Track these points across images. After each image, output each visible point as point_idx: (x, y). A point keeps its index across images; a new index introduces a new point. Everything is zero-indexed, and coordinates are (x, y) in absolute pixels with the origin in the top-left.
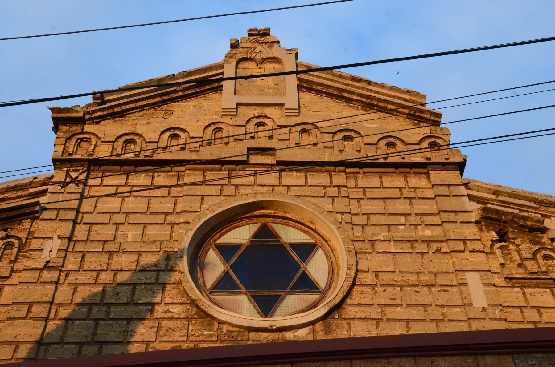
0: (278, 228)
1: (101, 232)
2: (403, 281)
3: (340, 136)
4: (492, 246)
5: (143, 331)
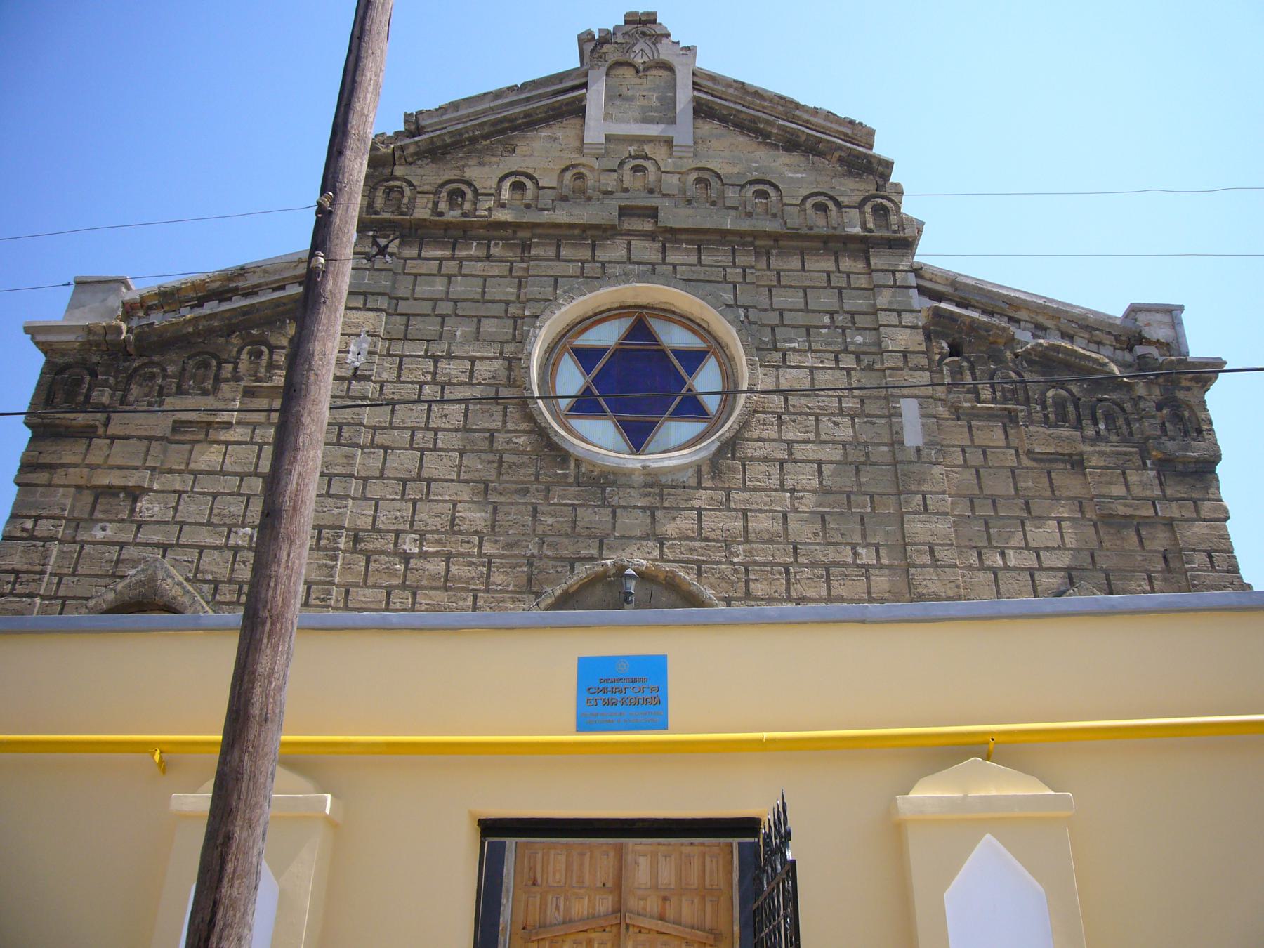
0: (657, 326)
1: (421, 327)
2: (819, 408)
3: (750, 190)
4: (942, 359)
5: (480, 466)
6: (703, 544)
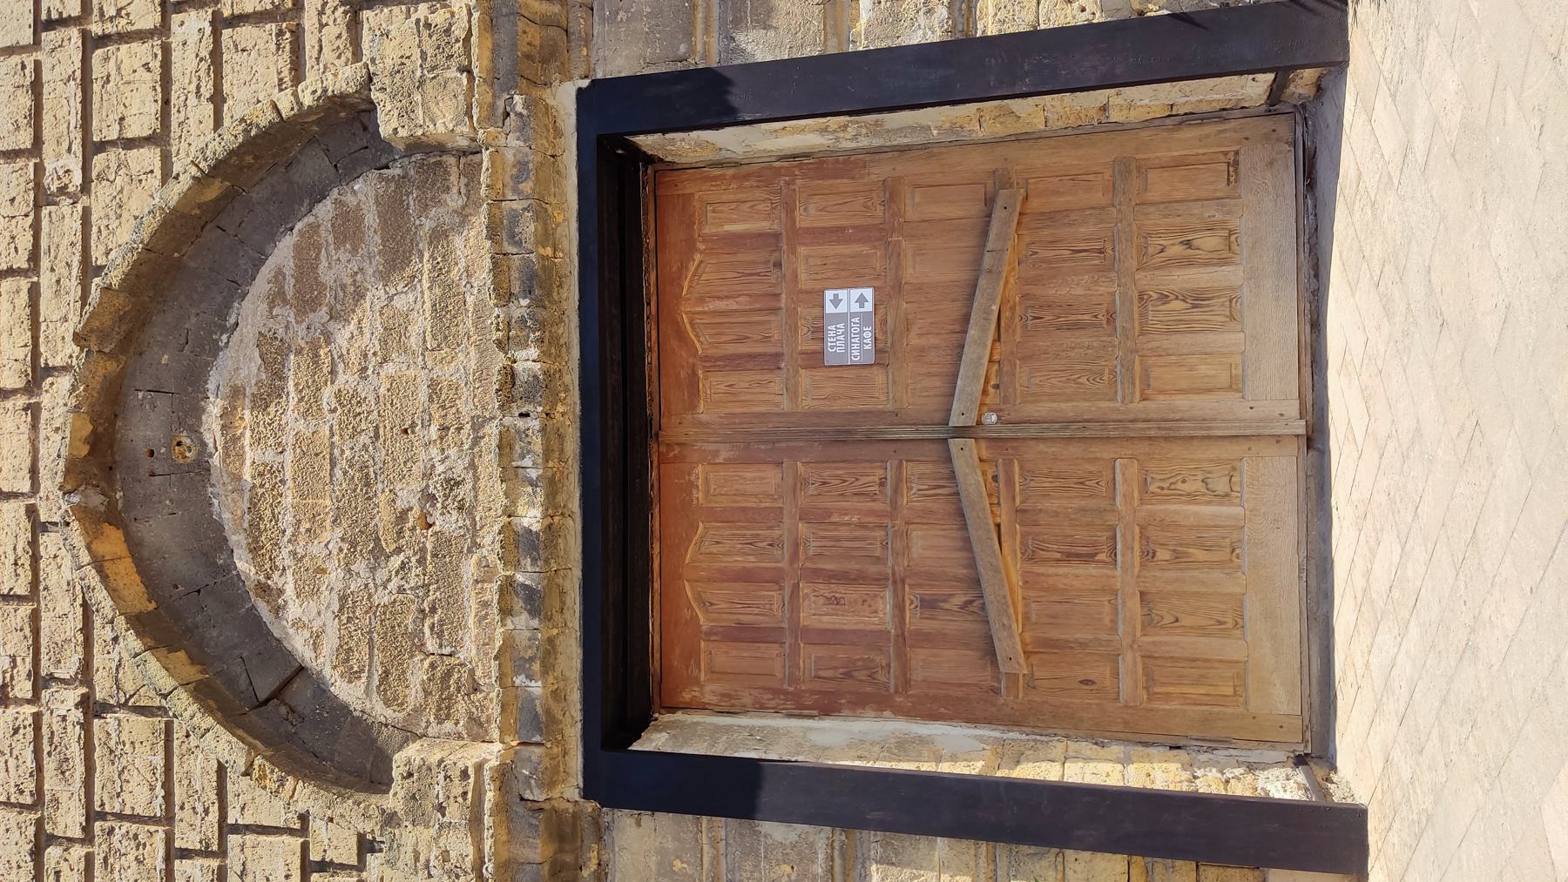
6: (45, 263)
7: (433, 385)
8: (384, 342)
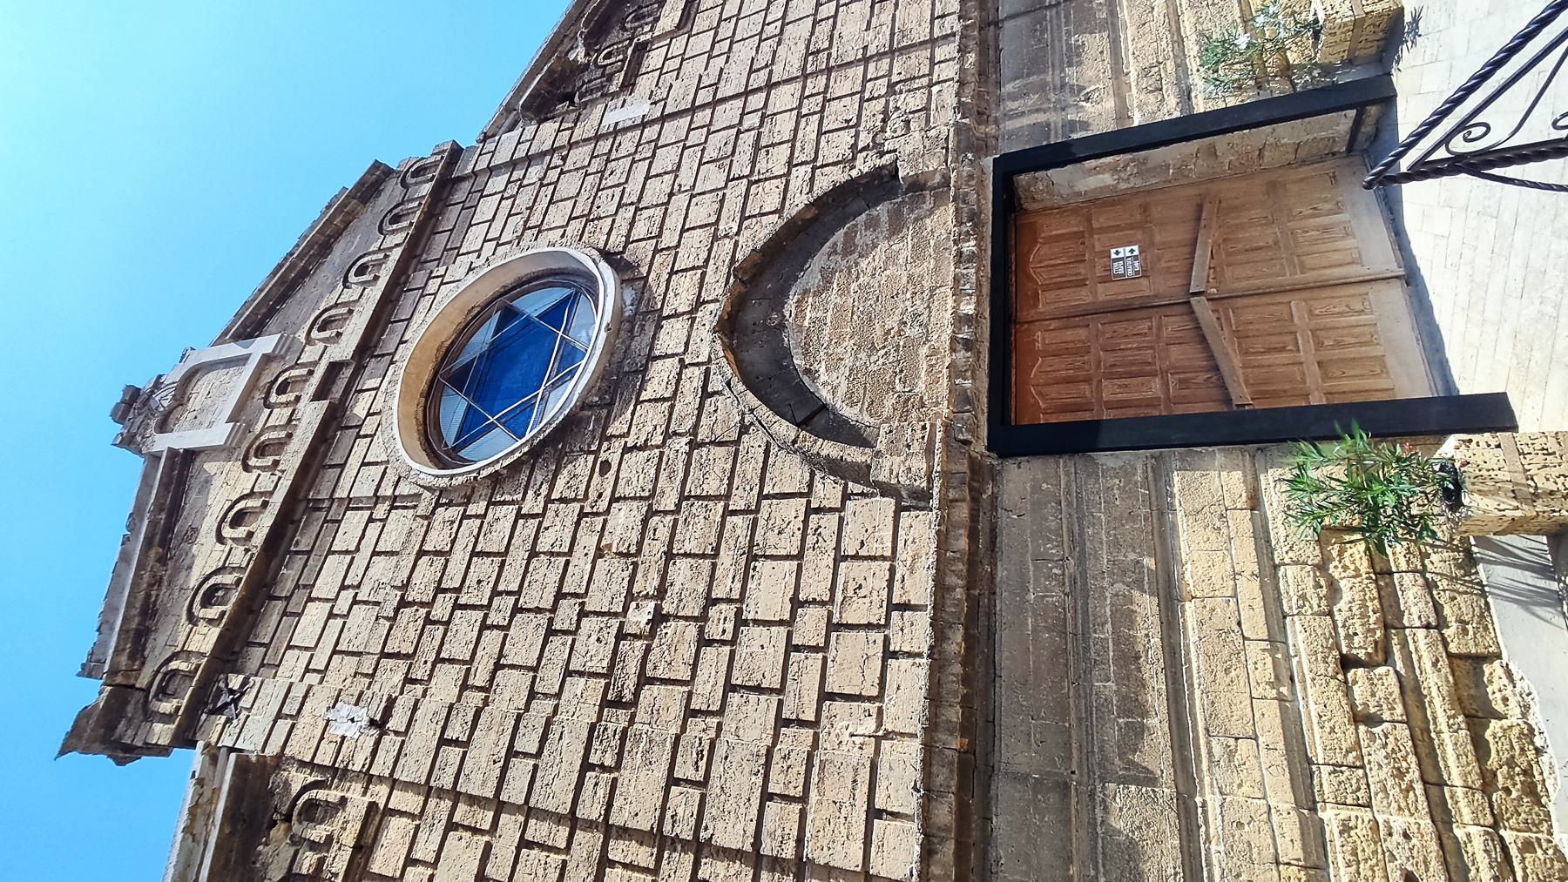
7: (910, 277)
8: (885, 263)
